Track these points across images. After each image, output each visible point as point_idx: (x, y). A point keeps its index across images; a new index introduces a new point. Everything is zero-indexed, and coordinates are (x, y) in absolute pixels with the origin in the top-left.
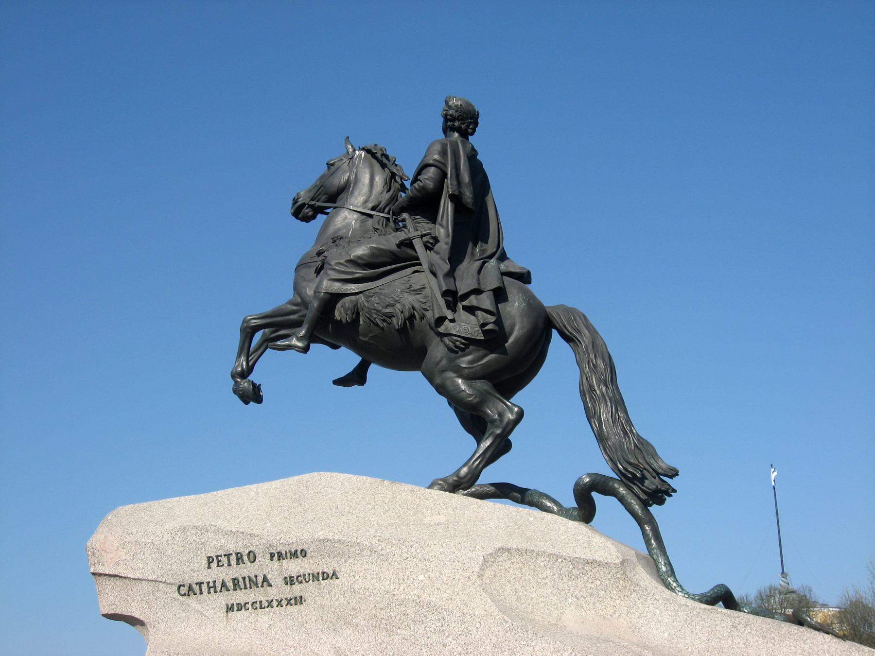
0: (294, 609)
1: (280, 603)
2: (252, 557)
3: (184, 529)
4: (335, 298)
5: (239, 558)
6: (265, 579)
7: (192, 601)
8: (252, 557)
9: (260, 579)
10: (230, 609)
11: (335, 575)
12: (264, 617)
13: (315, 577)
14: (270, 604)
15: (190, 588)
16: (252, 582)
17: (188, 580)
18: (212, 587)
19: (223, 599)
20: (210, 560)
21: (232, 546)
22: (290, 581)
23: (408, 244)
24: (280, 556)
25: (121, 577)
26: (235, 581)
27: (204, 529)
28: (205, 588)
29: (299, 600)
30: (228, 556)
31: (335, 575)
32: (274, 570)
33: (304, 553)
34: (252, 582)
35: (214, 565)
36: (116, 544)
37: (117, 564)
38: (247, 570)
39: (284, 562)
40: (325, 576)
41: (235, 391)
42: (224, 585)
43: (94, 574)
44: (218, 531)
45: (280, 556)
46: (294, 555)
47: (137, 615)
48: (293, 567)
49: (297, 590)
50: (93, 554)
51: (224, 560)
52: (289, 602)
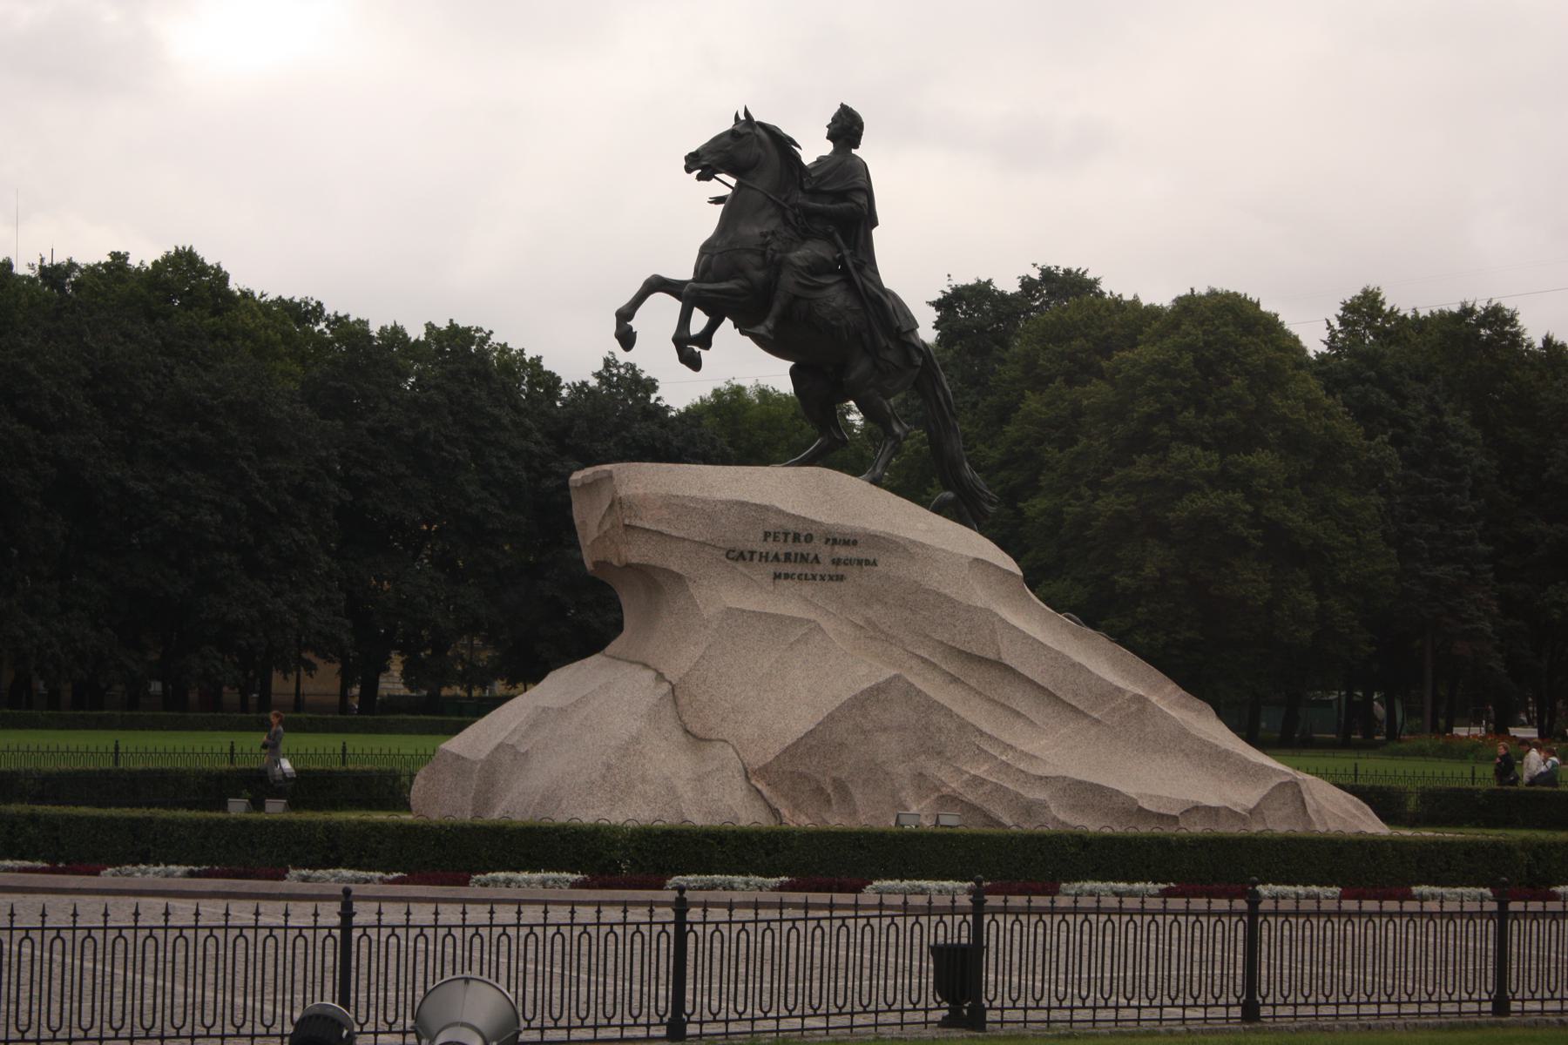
0: (834, 585)
1: (823, 578)
2: (809, 538)
3: (743, 504)
4: (796, 297)
5: (796, 537)
6: (816, 557)
7: (740, 566)
8: (809, 538)
9: (811, 557)
10: (777, 576)
11: (874, 563)
12: (807, 589)
13: (860, 562)
14: (814, 578)
15: (742, 554)
16: (804, 558)
17: (740, 546)
18: (764, 557)
19: (771, 568)
20: (767, 535)
21: (791, 526)
22: (836, 562)
23: (842, 260)
24: (835, 542)
25: (660, 533)
26: (787, 556)
27: (766, 508)
28: (756, 557)
29: (841, 578)
30: (786, 534)
31: (874, 563)
32: (825, 552)
33: (855, 543)
34: (804, 558)
35: (770, 539)
36: (659, 503)
37: (659, 521)
38: (802, 548)
39: (837, 548)
40: (867, 562)
41: (617, 336)
42: (776, 557)
43: (627, 527)
44: (779, 512)
45: (833, 540)
46: (846, 543)
47: (675, 569)
48: (842, 552)
49: (841, 569)
50: (630, 507)
51: (782, 537)
52: (831, 578)
